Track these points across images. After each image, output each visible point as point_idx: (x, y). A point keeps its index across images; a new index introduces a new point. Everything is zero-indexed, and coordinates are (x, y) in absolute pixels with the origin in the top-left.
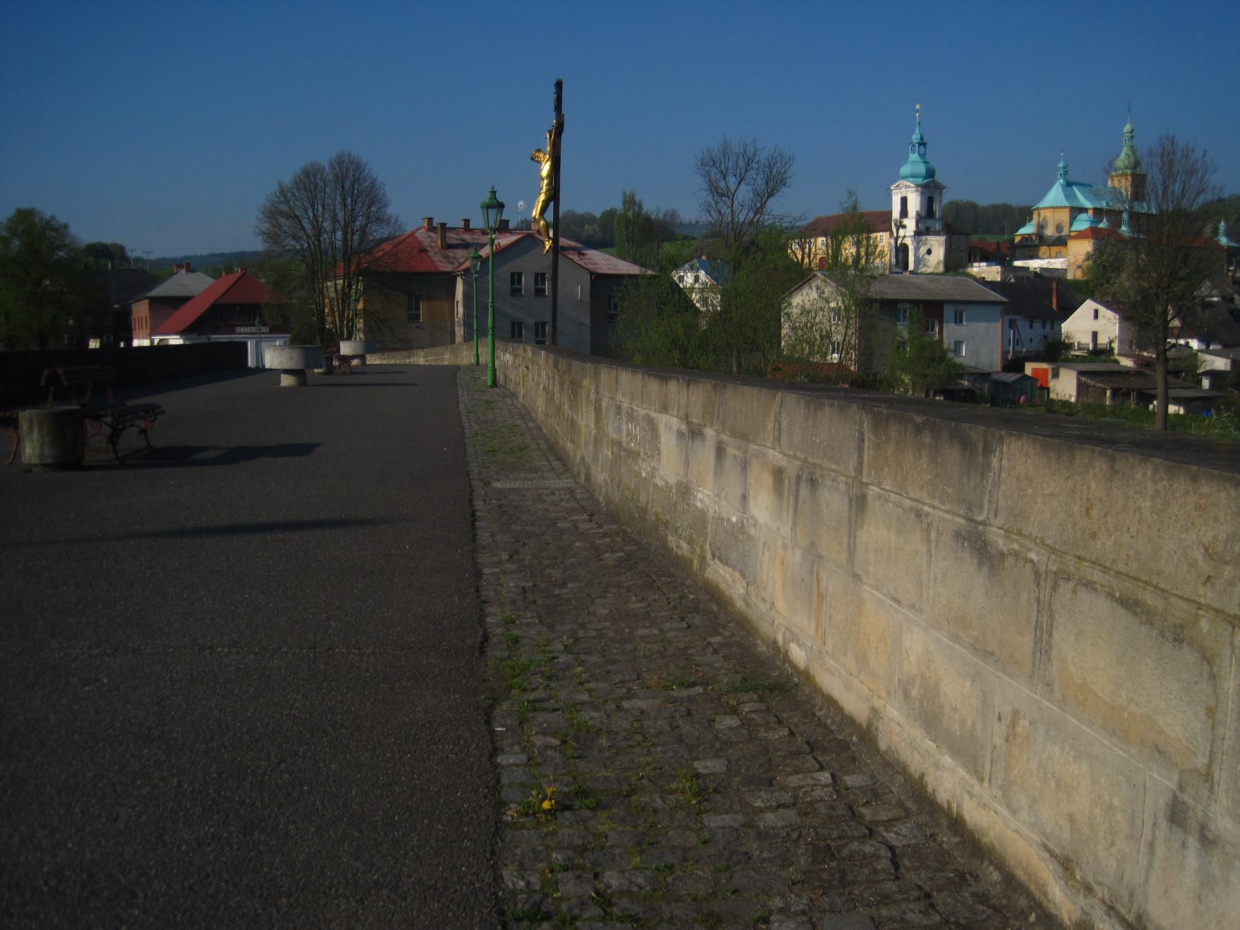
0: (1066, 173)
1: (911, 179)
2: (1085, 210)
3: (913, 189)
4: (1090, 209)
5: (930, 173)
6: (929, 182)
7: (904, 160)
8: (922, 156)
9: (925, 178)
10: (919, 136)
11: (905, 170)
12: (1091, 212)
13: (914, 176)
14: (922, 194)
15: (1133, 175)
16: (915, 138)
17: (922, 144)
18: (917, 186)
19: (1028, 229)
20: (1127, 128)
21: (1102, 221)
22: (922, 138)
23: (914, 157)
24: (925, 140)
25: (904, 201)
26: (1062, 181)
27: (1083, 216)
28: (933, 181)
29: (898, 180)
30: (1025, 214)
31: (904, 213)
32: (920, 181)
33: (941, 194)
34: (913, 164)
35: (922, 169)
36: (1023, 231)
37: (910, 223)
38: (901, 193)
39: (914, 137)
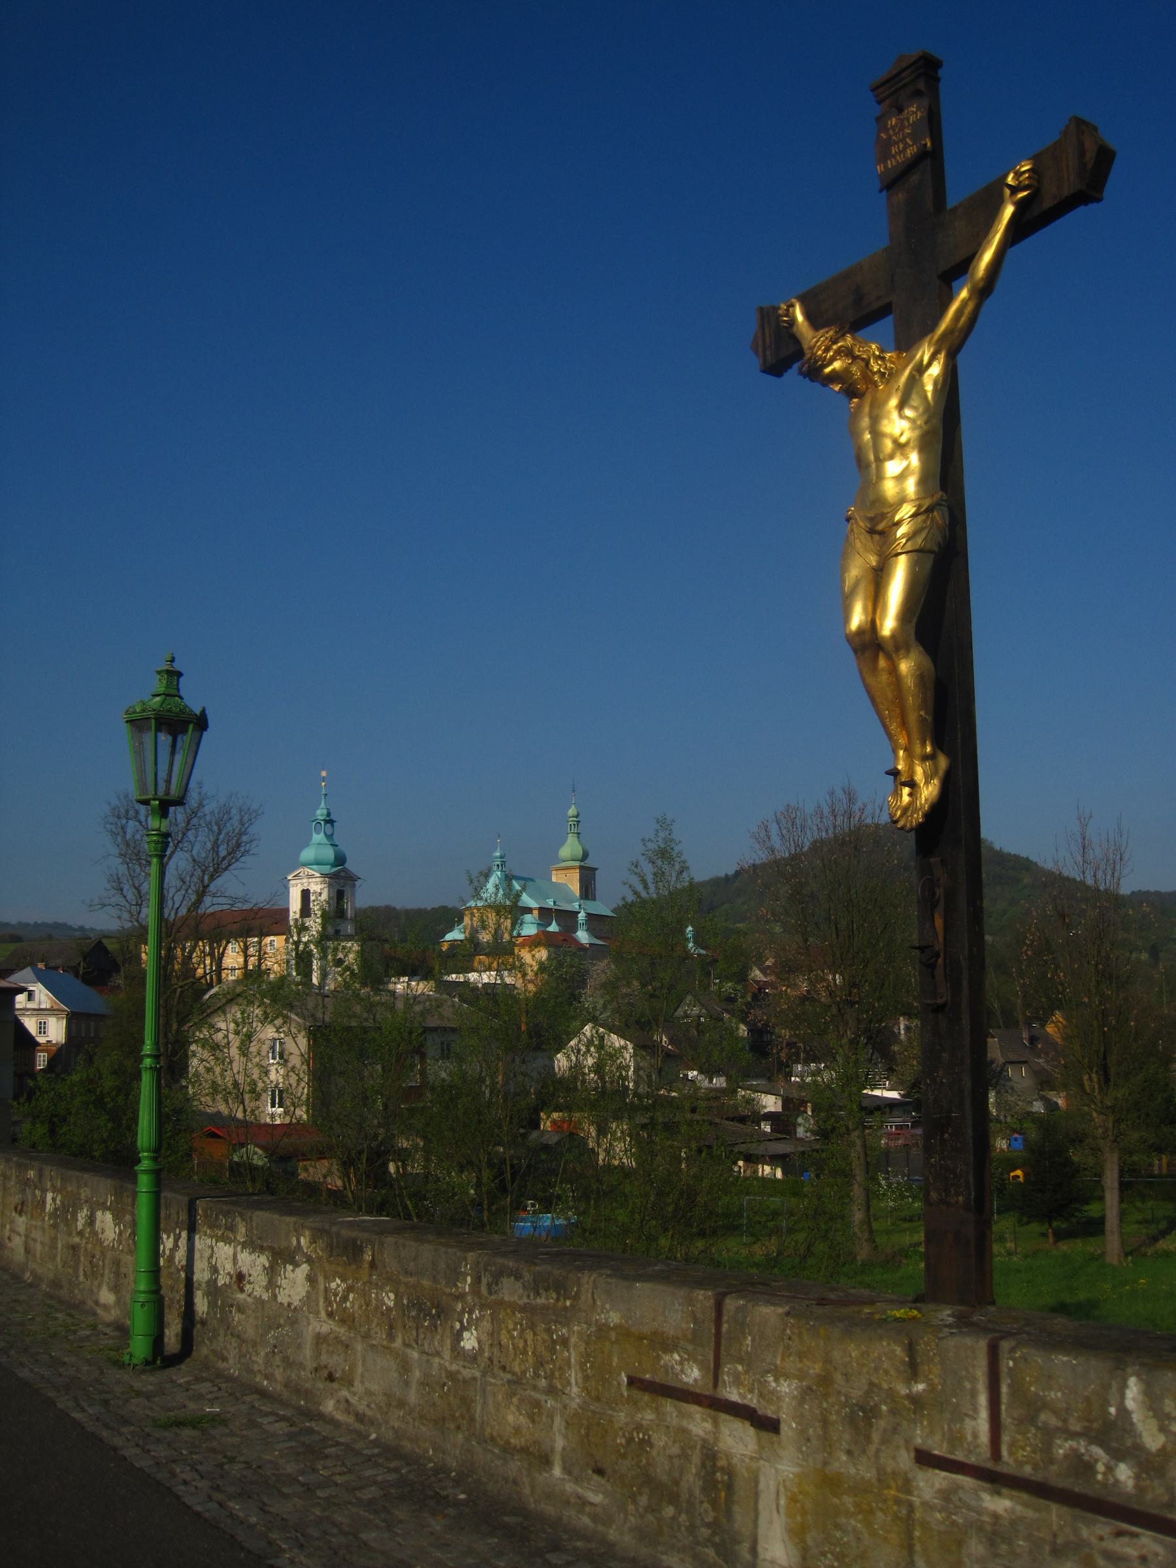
0: (503, 864)
1: (315, 867)
2: (529, 910)
3: (318, 879)
4: (535, 909)
5: (340, 860)
6: (339, 872)
7: (306, 843)
8: (329, 837)
9: (334, 866)
10: (325, 812)
11: (308, 854)
12: (536, 912)
13: (318, 863)
14: (330, 886)
15: (581, 868)
16: (321, 813)
17: (330, 821)
18: (324, 875)
19: (455, 935)
20: (572, 811)
21: (550, 924)
22: (329, 814)
23: (318, 837)
24: (333, 817)
25: (305, 894)
26: (499, 873)
27: (528, 917)
28: (344, 870)
29: (297, 868)
30: (451, 917)
31: (305, 911)
32: (327, 869)
33: (354, 886)
34: (317, 847)
35: (329, 854)
36: (449, 937)
37: (314, 924)
38: (302, 884)
39: (319, 812)
